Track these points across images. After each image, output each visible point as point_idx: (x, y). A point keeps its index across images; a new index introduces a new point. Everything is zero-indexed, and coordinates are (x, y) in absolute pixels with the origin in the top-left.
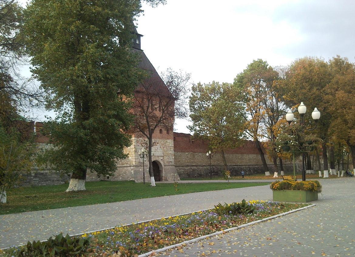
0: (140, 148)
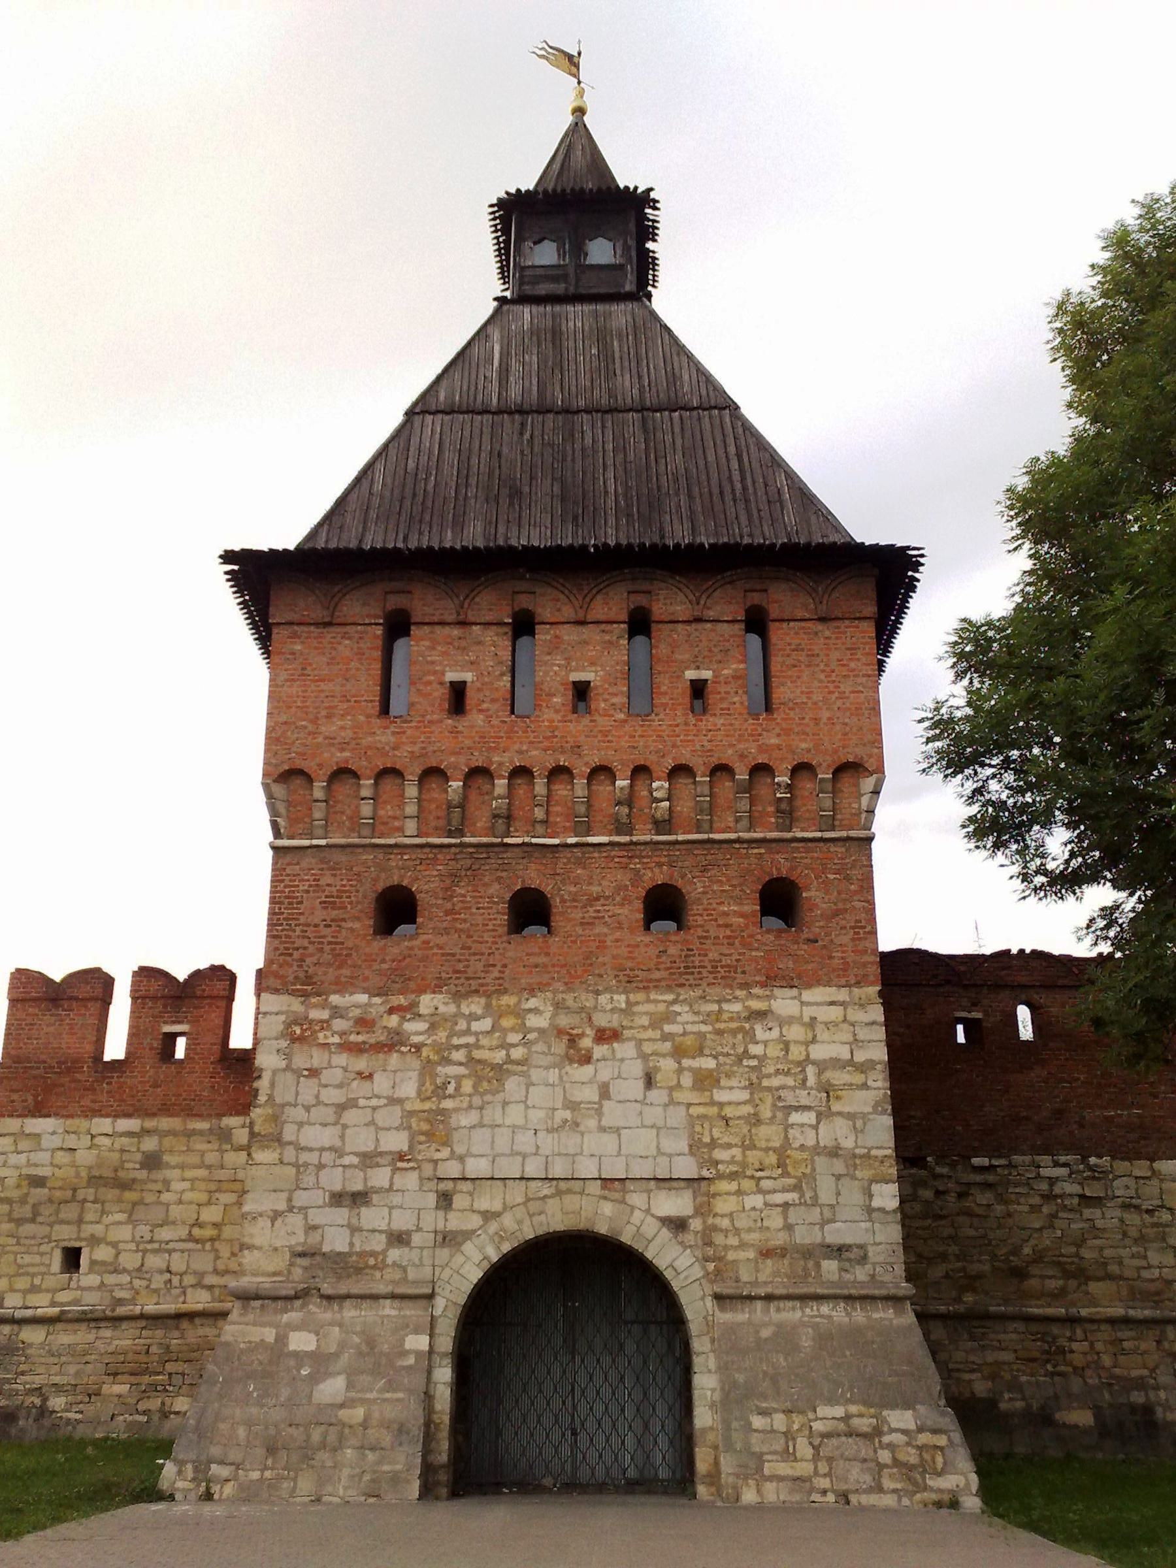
0: (333, 1096)
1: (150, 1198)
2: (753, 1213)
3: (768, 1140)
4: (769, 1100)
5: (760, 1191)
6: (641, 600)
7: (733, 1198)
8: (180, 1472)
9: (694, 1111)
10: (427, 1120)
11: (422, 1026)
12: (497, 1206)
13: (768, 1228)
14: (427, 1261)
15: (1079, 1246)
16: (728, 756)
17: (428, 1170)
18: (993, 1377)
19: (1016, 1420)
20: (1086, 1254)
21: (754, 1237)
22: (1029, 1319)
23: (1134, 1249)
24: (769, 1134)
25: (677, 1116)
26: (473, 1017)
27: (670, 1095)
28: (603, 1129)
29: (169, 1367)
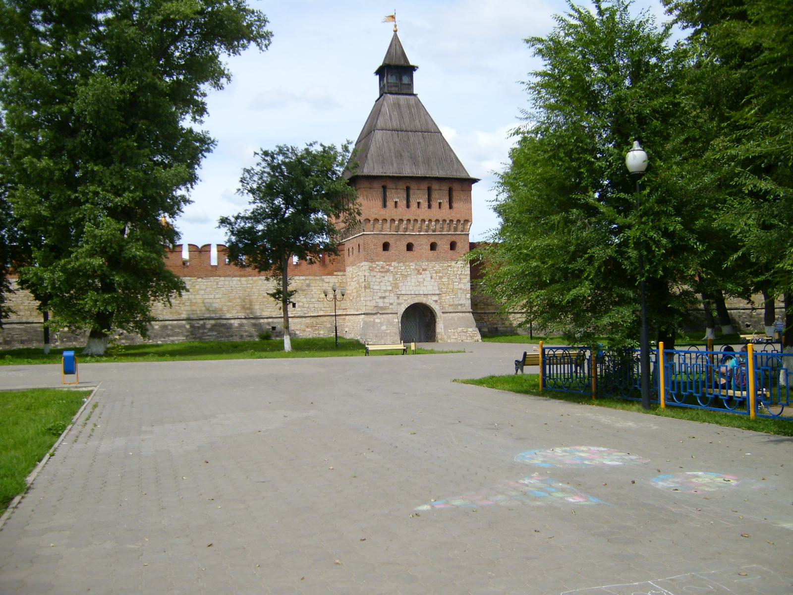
1: (309, 293)
6: (430, 185)
11: (392, 268)
16: (445, 218)
20: (489, 301)
22: (477, 313)
24: (451, 286)
25: (436, 284)
26: (401, 266)
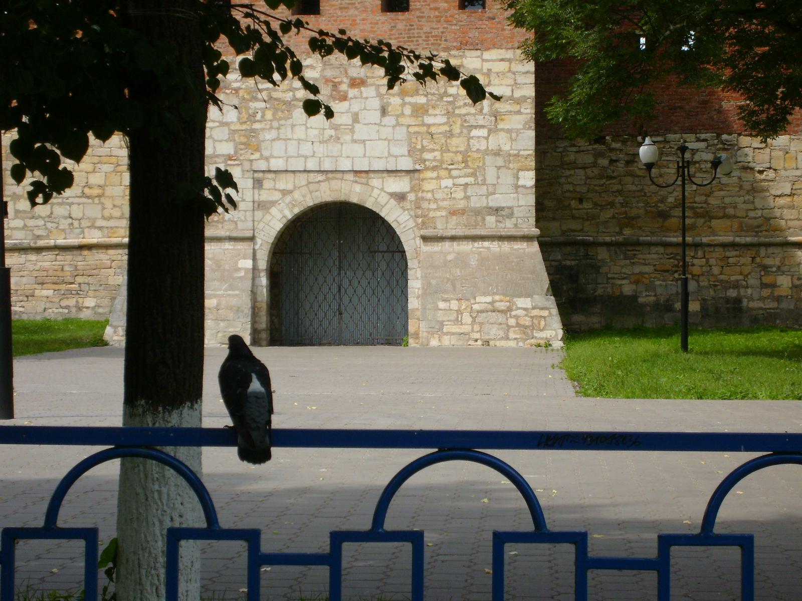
2: (446, 190)
3: (457, 147)
4: (459, 122)
5: (451, 177)
7: (434, 181)
8: (115, 332)
9: (412, 129)
10: (245, 136)
12: (290, 187)
13: (454, 198)
14: (250, 219)
15: (708, 196)
17: (247, 165)
18: (637, 282)
19: (648, 309)
20: (712, 201)
21: (446, 204)
23: (747, 197)
24: (458, 143)
25: (401, 133)
27: (397, 120)
28: (354, 141)
29: (79, 279)
